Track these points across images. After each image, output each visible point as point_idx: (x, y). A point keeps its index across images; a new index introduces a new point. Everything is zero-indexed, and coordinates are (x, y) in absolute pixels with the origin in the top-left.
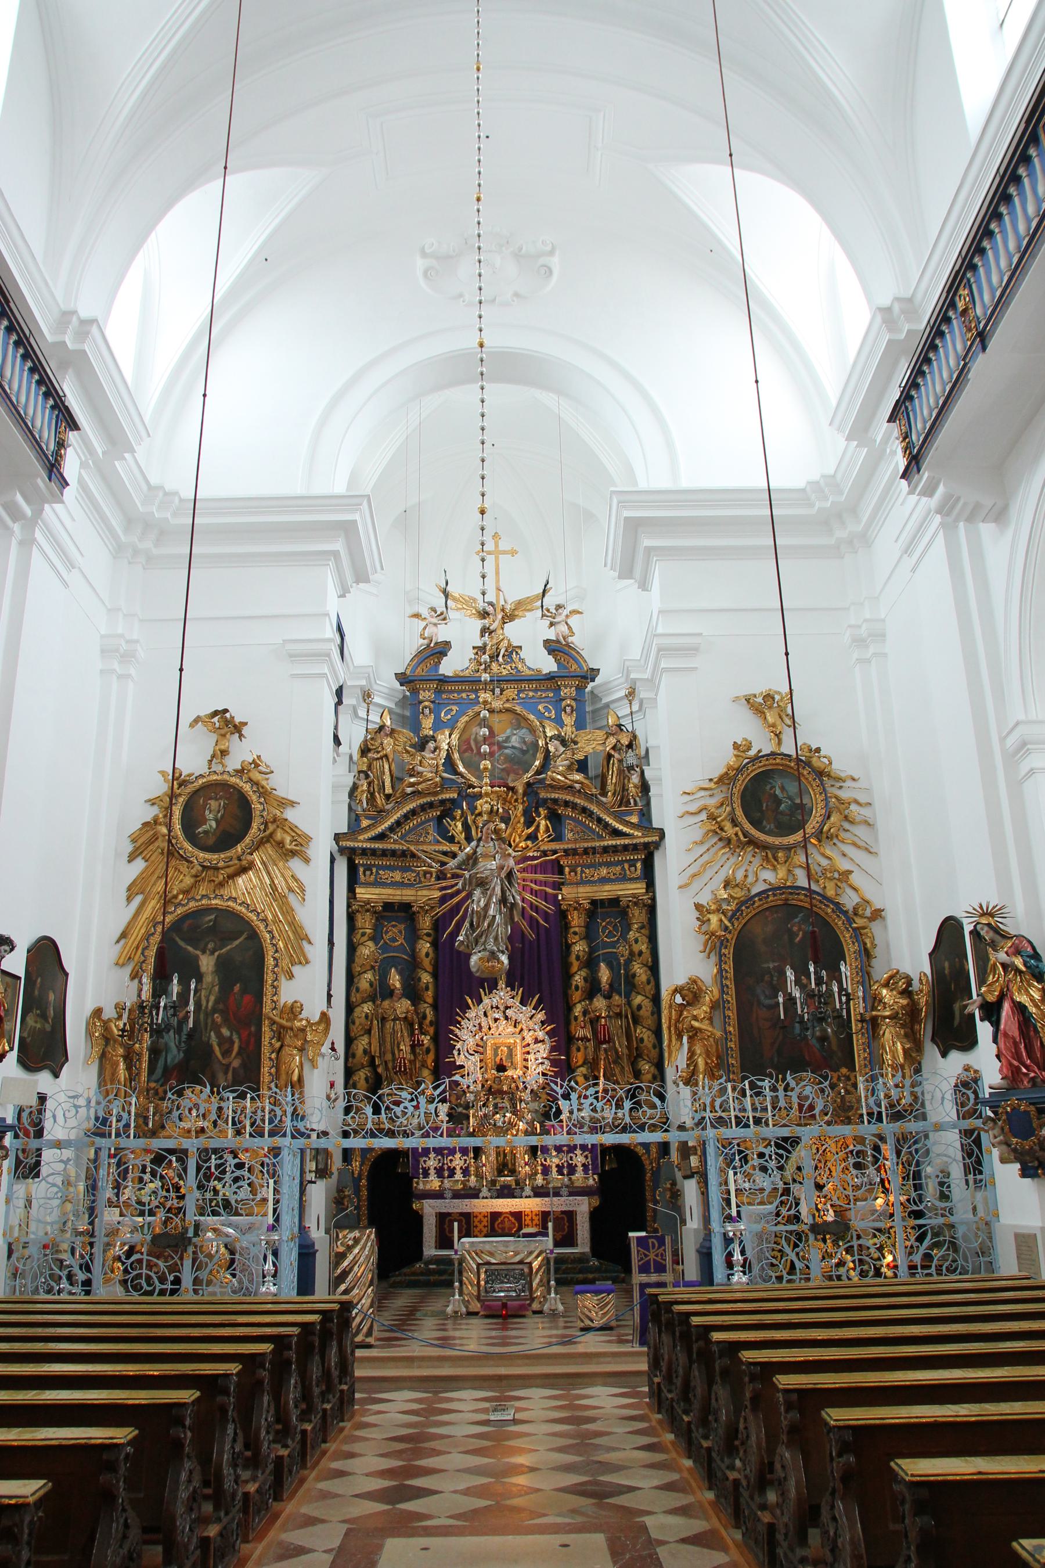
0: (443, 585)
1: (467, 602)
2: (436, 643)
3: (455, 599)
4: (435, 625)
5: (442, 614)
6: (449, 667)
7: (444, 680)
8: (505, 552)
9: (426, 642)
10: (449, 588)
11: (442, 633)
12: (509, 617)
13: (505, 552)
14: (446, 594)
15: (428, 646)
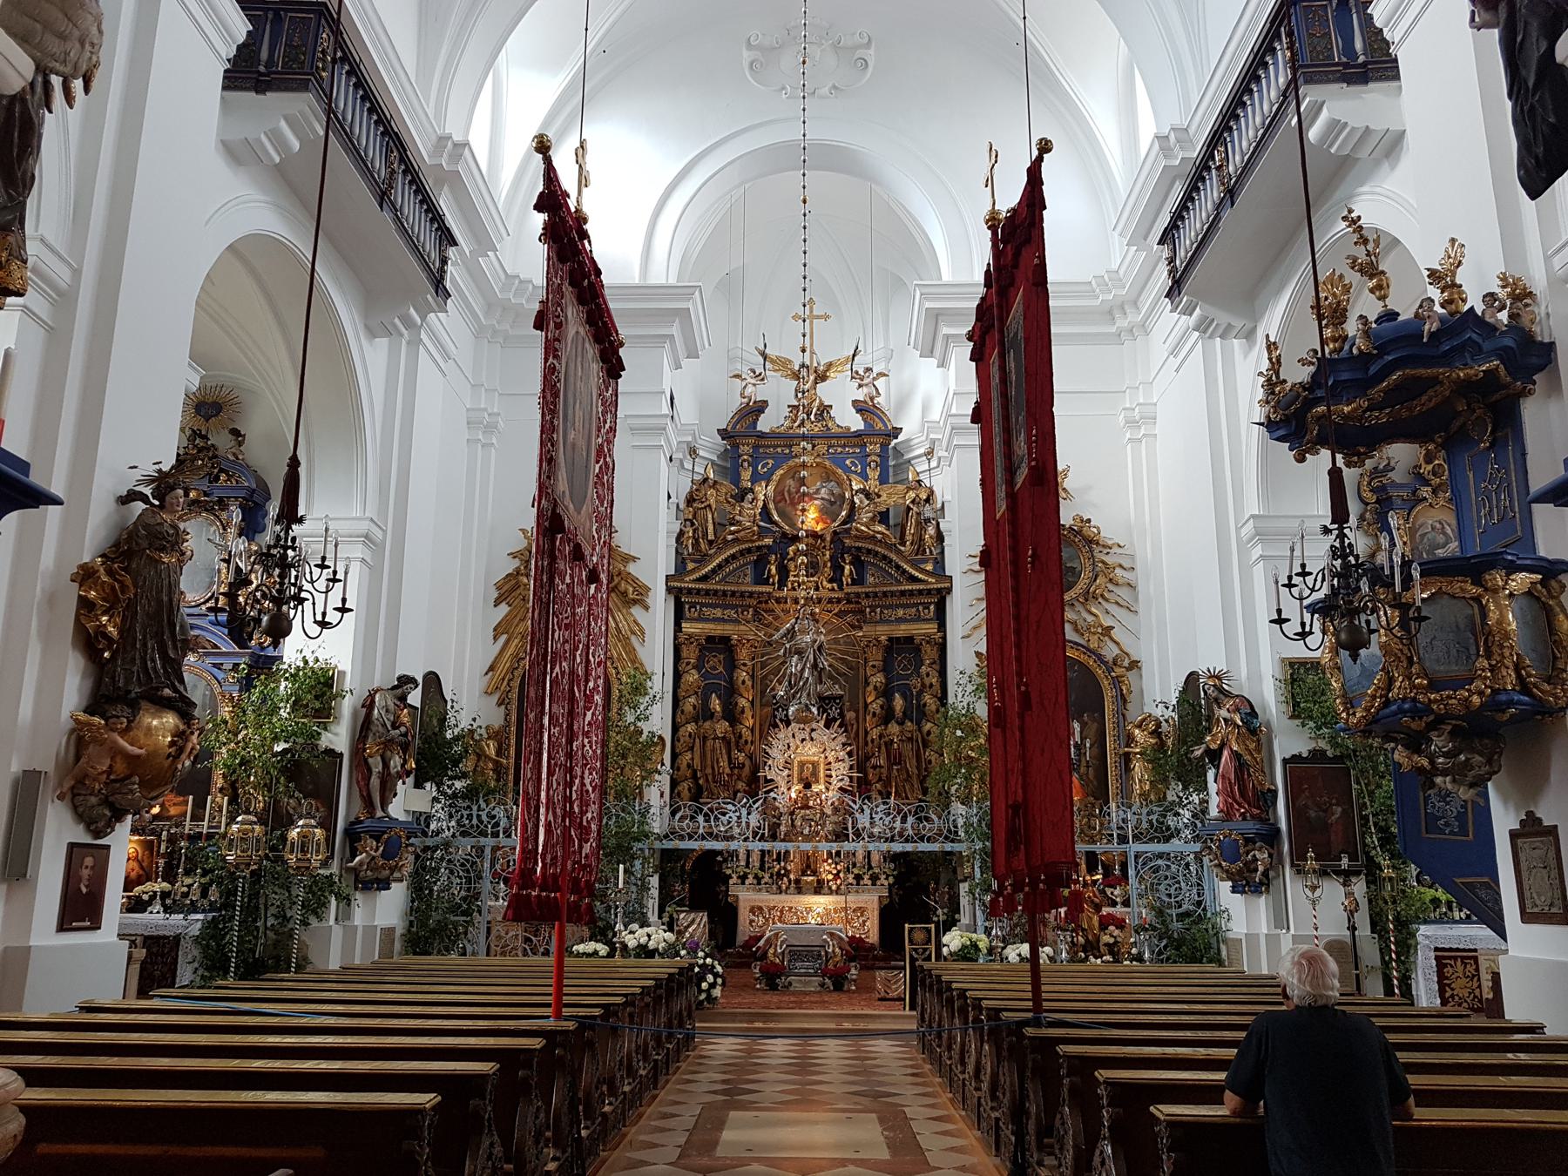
0: (761, 347)
1: (782, 364)
2: (755, 402)
3: (772, 362)
4: (754, 385)
5: (760, 374)
6: (765, 424)
7: (762, 435)
8: (818, 317)
9: (746, 400)
10: (767, 351)
11: (759, 393)
12: (822, 377)
13: (818, 317)
14: (765, 357)
15: (748, 404)
